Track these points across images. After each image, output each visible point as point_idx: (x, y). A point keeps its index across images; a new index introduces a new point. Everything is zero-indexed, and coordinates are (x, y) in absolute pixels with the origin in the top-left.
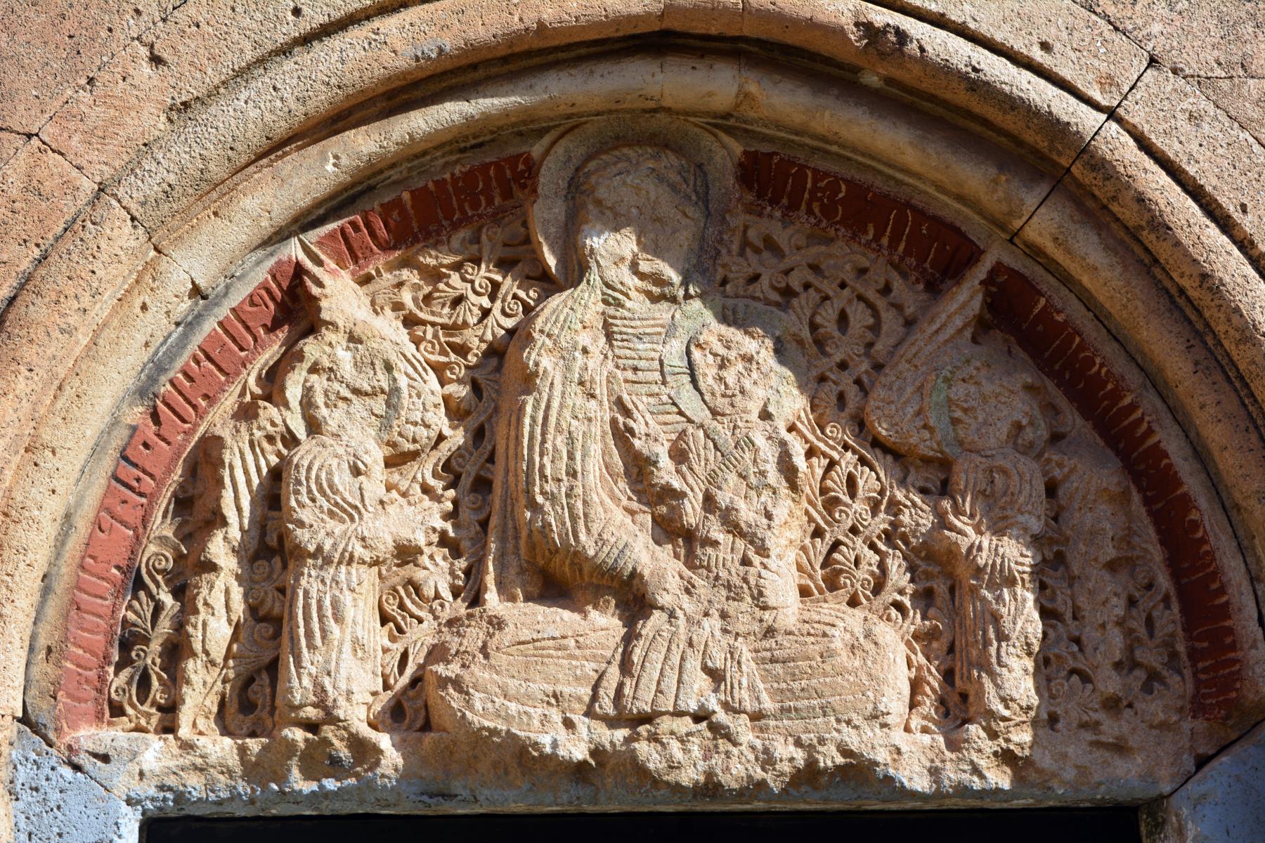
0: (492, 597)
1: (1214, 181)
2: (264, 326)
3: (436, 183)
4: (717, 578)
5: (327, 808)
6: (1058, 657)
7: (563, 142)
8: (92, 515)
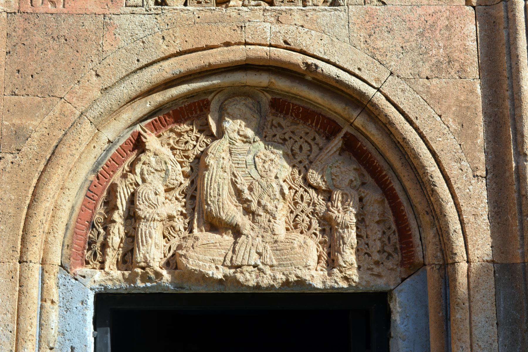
0: (196, 231)
1: (408, 110)
2: (130, 150)
3: (180, 108)
4: (261, 226)
5: (148, 291)
6: (361, 249)
7: (218, 95)
8: (80, 207)
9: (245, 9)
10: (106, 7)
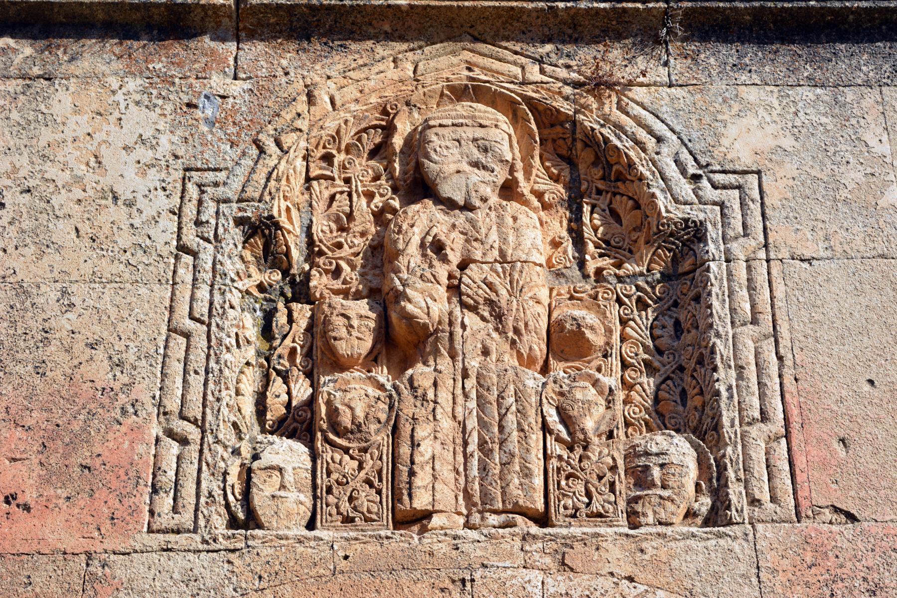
9: (473, 534)
10: (96, 534)
